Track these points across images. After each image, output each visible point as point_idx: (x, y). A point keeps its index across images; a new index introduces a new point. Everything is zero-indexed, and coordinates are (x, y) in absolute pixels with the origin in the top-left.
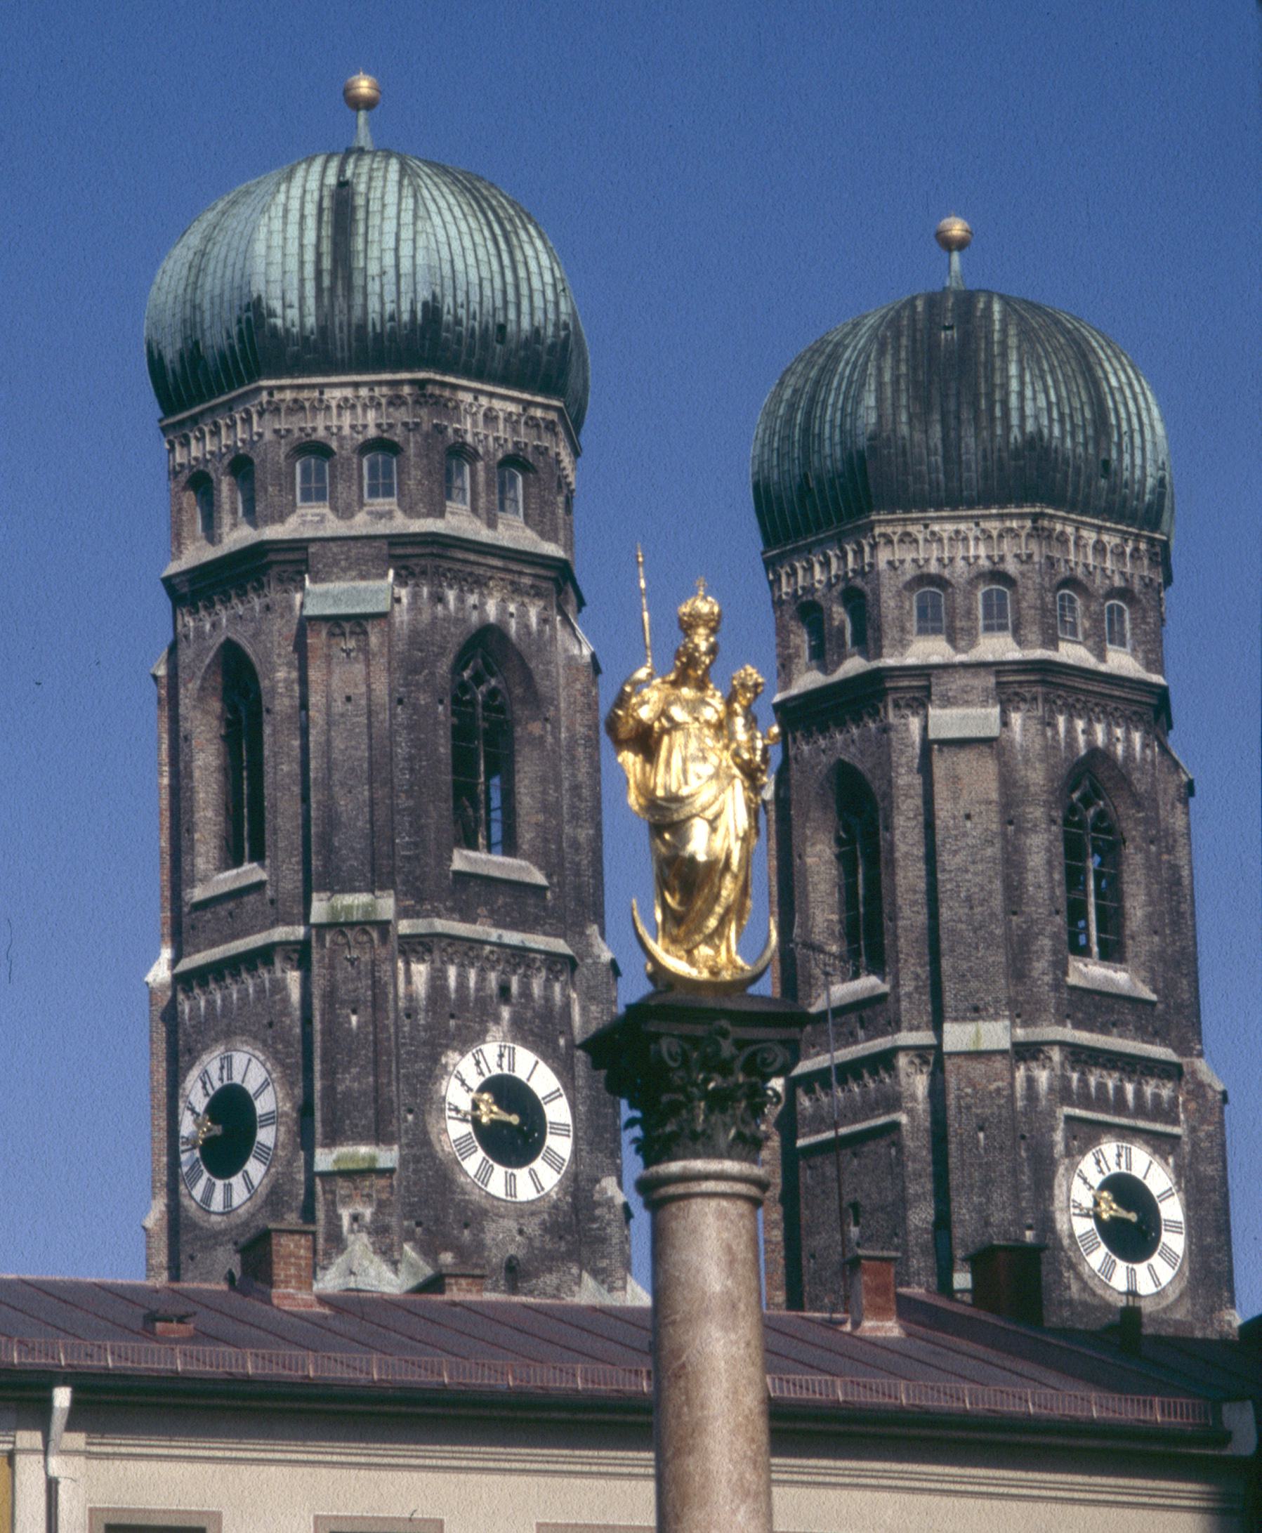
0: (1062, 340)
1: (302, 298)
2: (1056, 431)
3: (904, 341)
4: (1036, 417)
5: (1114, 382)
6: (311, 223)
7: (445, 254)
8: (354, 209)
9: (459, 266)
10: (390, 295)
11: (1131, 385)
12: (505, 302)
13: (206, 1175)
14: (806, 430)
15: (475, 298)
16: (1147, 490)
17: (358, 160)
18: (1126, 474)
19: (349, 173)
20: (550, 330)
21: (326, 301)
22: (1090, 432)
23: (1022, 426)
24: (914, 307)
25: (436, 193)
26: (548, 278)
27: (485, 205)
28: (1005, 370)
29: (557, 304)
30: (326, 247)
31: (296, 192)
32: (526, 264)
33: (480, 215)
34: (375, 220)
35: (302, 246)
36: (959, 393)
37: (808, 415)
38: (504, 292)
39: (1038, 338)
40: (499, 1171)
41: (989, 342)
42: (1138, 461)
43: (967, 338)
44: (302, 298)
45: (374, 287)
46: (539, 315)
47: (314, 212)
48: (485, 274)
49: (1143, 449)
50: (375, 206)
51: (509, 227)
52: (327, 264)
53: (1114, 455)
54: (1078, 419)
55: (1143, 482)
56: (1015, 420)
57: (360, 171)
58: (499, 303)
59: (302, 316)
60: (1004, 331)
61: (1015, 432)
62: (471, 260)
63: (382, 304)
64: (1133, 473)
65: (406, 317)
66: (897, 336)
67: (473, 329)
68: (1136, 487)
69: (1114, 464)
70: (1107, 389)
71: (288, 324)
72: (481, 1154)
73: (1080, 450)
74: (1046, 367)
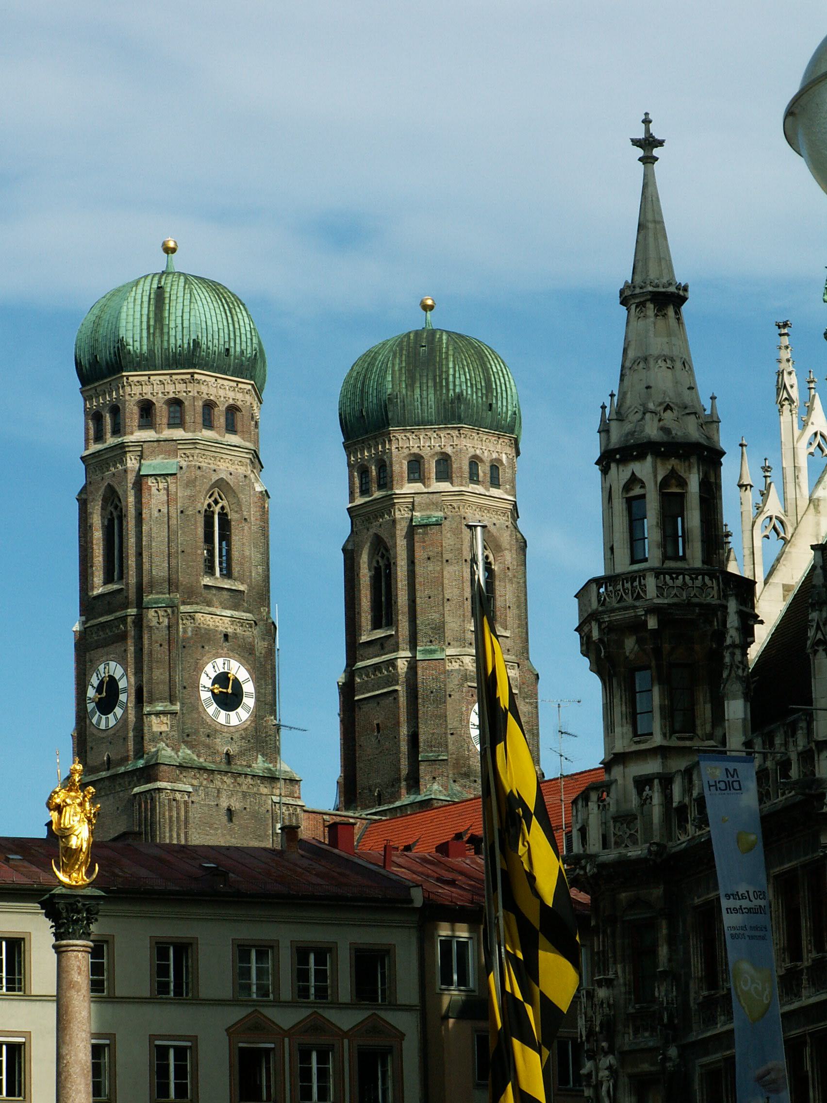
0: (473, 351)
1: (141, 338)
2: (469, 392)
3: (404, 352)
4: (460, 386)
5: (495, 370)
6: (145, 305)
7: (203, 319)
8: (164, 299)
9: (209, 323)
10: (179, 336)
11: (502, 371)
12: (229, 338)
13: (98, 713)
14: (362, 391)
17: (166, 277)
18: (499, 410)
19: (162, 283)
20: (249, 351)
21: (152, 339)
22: (484, 392)
23: (454, 390)
24: (409, 337)
25: (200, 291)
26: (248, 328)
27: (221, 296)
28: (447, 365)
29: (252, 339)
30: (152, 315)
31: (139, 291)
32: (239, 322)
33: (219, 301)
34: (173, 304)
35: (141, 315)
36: (427, 376)
37: (363, 383)
38: (229, 335)
39: (462, 350)
40: (223, 712)
41: (441, 353)
42: (505, 404)
43: (432, 351)
44: (141, 338)
45: (172, 333)
46: (244, 344)
47: (147, 300)
48: (221, 327)
49: (507, 399)
50: (173, 297)
51: (231, 306)
52: (152, 322)
53: (494, 402)
55: (507, 413)
56: (451, 387)
57: (166, 282)
58: (227, 340)
59: (141, 345)
60: (447, 348)
61: (451, 392)
62: (214, 321)
63: (176, 340)
64: (502, 409)
65: (186, 346)
66: (401, 350)
67: (215, 351)
69: (494, 406)
70: (491, 373)
71: (135, 349)
72: (215, 705)
73: (480, 399)
74: (465, 364)
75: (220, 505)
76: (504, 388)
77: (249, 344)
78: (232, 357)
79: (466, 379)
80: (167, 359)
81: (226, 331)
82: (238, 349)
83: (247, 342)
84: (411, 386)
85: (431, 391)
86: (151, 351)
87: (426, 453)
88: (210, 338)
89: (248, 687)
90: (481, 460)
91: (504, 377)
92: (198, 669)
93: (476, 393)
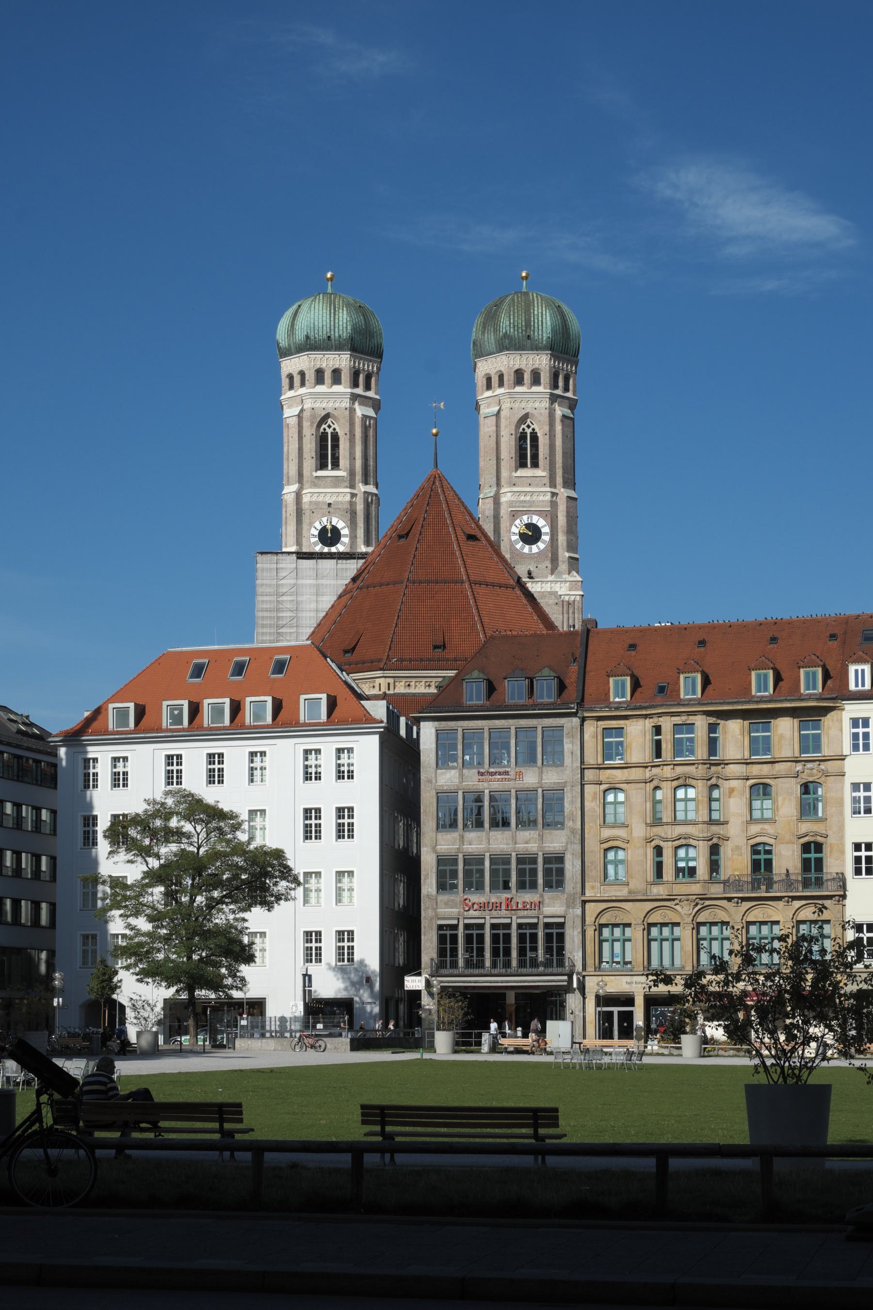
2: (512, 331)
7: (312, 321)
9: (316, 323)
15: (321, 330)
22: (524, 328)
26: (345, 321)
46: (341, 332)
48: (324, 323)
58: (328, 330)
69: (532, 336)
73: (520, 334)
76: (540, 323)
79: (510, 323)
80: (296, 348)
81: (328, 326)
82: (337, 335)
84: (483, 333)
85: (492, 334)
86: (289, 345)
89: (345, 532)
91: (542, 317)
92: (311, 524)
93: (518, 330)
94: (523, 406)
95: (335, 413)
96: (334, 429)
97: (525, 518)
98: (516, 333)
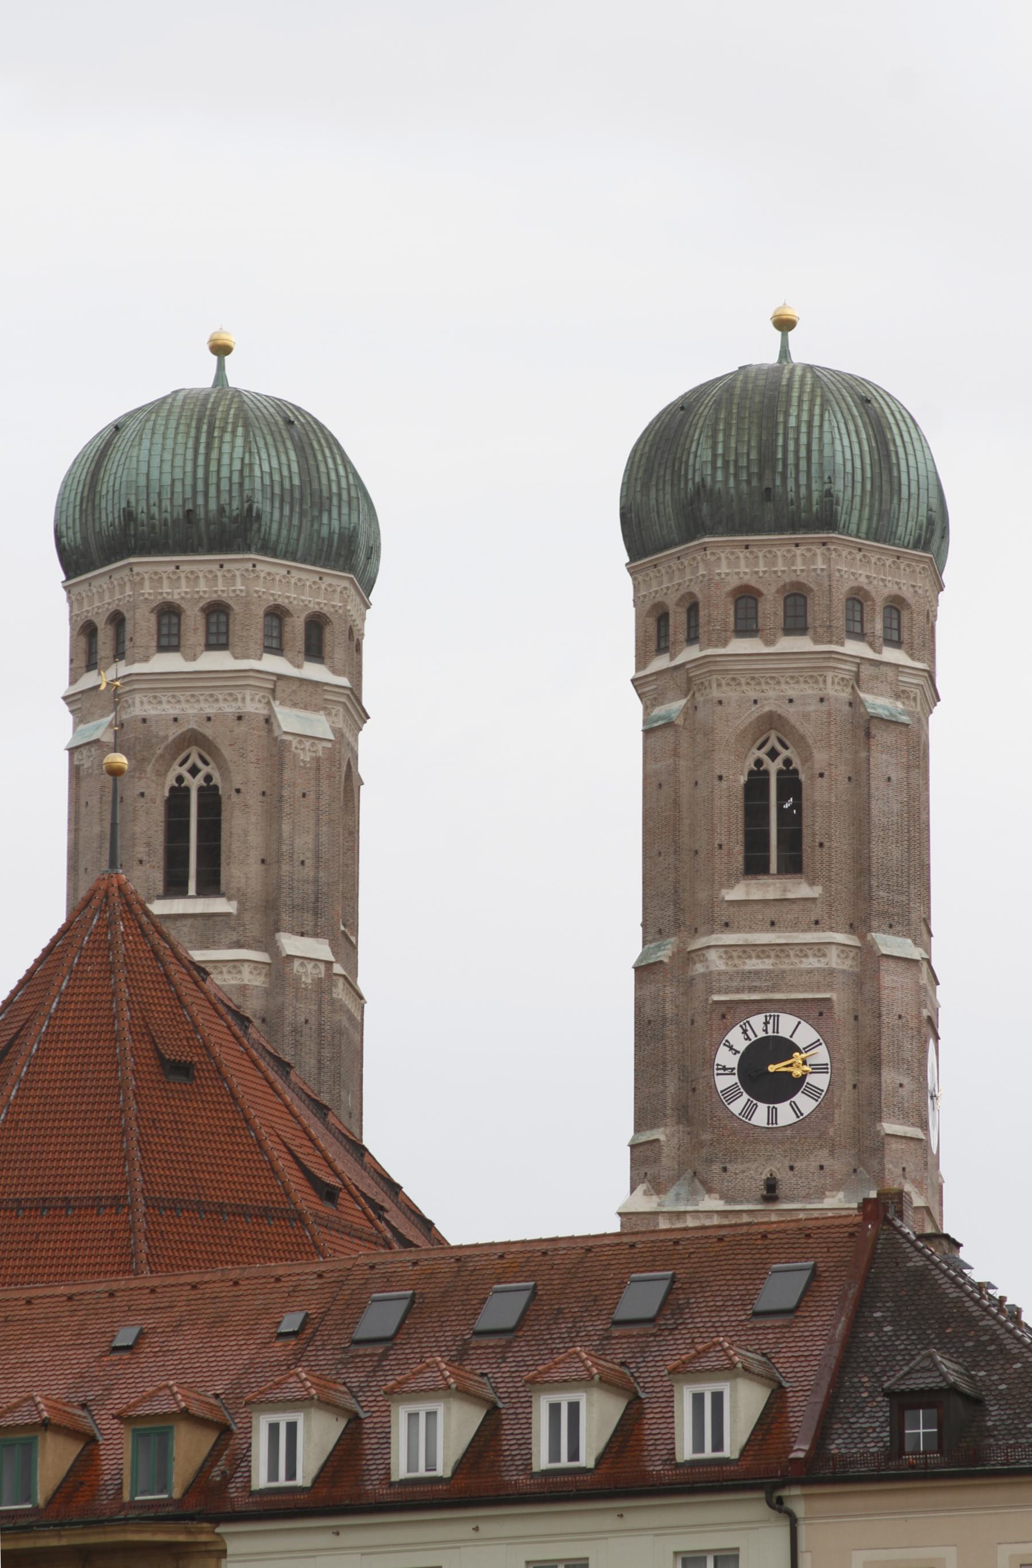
1: (74, 520)
2: (720, 476)
7: (143, 469)
9: (155, 474)
15: (166, 495)
16: (814, 502)
18: (791, 495)
20: (235, 504)
22: (755, 469)
26: (237, 465)
29: (241, 485)
38: (194, 486)
42: (803, 480)
46: (225, 498)
53: (778, 482)
54: (743, 462)
58: (189, 494)
59: (74, 533)
64: (798, 492)
67: (166, 520)
68: (803, 502)
69: (779, 490)
73: (744, 486)
75: (200, 776)
76: (803, 453)
77: (235, 493)
78: (202, 524)
79: (715, 456)
81: (189, 481)
83: (230, 491)
85: (668, 489)
87: (672, 601)
88: (154, 498)
90: (759, 594)
93: (736, 475)
94: (753, 695)
95: (208, 731)
96: (208, 778)
97: (757, 1021)
98: (732, 483)
